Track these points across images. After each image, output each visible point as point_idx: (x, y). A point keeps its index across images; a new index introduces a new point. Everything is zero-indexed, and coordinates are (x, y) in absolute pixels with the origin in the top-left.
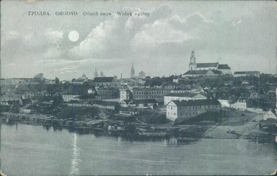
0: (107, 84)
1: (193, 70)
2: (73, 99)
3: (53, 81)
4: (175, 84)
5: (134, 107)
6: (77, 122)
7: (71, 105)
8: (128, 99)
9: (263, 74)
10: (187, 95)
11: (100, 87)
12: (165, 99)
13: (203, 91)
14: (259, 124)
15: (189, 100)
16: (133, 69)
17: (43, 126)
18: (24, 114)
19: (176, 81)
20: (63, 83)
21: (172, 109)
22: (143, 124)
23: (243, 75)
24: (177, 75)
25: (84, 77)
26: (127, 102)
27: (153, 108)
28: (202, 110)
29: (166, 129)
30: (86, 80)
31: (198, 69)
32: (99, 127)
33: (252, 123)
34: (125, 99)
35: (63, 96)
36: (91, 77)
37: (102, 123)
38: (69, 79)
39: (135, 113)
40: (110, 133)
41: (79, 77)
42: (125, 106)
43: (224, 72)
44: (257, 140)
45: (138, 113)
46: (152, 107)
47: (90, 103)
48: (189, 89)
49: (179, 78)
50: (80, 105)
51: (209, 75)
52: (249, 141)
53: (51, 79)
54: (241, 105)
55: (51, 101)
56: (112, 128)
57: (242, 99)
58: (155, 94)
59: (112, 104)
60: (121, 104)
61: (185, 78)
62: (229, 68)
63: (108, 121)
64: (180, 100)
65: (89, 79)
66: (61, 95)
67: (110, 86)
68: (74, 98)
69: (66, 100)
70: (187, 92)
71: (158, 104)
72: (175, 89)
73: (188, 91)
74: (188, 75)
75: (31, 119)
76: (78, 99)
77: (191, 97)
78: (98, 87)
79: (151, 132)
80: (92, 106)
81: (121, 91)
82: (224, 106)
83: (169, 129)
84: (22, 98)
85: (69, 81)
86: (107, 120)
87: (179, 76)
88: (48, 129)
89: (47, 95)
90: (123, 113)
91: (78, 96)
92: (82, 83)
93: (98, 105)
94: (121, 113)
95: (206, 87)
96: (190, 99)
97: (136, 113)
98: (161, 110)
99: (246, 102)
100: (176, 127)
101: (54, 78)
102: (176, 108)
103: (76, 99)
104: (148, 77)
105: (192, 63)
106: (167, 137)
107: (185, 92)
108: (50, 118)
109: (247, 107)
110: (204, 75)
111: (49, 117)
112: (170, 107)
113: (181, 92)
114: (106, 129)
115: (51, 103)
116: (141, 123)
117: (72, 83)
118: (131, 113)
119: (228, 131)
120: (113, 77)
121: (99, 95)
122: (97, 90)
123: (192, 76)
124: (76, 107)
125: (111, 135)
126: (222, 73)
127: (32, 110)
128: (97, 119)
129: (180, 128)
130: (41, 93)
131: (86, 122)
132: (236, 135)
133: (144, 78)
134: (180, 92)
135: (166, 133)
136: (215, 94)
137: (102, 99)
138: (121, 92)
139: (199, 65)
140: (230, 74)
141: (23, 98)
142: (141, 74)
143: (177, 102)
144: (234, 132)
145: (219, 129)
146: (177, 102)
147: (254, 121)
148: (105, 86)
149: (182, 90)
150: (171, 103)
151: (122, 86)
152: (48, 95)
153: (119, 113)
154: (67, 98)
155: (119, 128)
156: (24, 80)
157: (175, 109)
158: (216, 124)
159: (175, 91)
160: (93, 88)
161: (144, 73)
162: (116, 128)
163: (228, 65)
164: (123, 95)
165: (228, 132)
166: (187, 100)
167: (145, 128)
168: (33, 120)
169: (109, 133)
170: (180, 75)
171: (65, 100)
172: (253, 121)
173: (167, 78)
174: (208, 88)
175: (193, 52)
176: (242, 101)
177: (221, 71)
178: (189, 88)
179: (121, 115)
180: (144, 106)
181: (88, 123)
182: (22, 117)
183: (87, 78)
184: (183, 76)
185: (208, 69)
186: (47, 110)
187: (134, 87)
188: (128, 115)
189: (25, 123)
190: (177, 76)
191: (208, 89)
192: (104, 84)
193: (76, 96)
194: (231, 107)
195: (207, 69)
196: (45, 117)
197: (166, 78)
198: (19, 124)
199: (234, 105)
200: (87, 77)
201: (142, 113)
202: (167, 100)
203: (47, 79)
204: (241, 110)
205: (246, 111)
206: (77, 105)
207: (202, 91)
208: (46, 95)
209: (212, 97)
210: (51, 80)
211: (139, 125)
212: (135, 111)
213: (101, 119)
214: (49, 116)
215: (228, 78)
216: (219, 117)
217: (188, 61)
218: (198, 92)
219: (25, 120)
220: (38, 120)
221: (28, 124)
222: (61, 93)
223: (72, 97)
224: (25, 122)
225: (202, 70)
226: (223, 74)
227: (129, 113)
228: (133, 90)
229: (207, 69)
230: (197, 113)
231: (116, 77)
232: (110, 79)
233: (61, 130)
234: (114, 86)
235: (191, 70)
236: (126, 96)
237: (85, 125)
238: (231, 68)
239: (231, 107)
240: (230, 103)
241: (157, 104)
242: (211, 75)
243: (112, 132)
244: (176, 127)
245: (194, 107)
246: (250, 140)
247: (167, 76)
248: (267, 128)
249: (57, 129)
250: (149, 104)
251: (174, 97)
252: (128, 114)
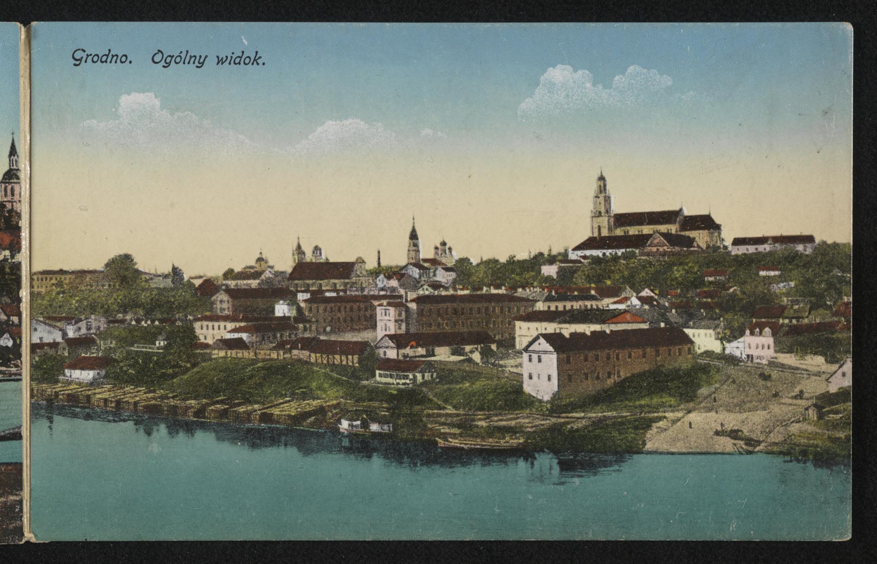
0: (335, 284)
1: (603, 235)
2: (229, 336)
3: (166, 276)
4: (549, 279)
5: (422, 356)
6: (242, 409)
7: (222, 354)
8: (399, 332)
9: (824, 243)
11: (313, 293)
12: (517, 328)
13: (635, 301)
14: (815, 405)
15: (593, 333)
16: (414, 236)
17: (136, 424)
18: (71, 387)
19: (550, 271)
20: (197, 283)
21: (540, 361)
22: (450, 410)
23: (761, 248)
24: (554, 253)
25: (262, 263)
26: (399, 341)
27: (482, 359)
28: (632, 364)
29: (522, 427)
30: (268, 274)
31: (619, 232)
32: (312, 425)
33: (795, 401)
34: (392, 332)
35: (197, 325)
37: (321, 411)
38: (215, 271)
39: (423, 377)
40: (346, 443)
41: (243, 266)
42: (392, 354)
43: (701, 238)
44: (811, 457)
45: (435, 375)
46: (477, 357)
47: (281, 346)
48: (593, 298)
49: (561, 261)
50: (248, 355)
52: (785, 462)
53: (159, 273)
54: (756, 346)
55: (157, 342)
56: (351, 426)
57: (762, 327)
59: (347, 348)
60: (380, 347)
61: (580, 262)
62: (718, 227)
63: (338, 404)
64: (566, 334)
65: (277, 268)
66: (191, 322)
67: (345, 291)
69: (205, 338)
70: (586, 306)
71: (498, 348)
72: (549, 299)
73: (588, 304)
74: (588, 253)
75: (94, 400)
76: (244, 336)
77: (603, 322)
78: (307, 296)
79: (476, 436)
80: (288, 356)
81: (379, 305)
82: (702, 350)
83: (531, 427)
84: (64, 334)
85: (217, 278)
86: (335, 402)
87: (560, 254)
88: (149, 433)
89: (146, 322)
90: (386, 376)
91: (243, 324)
92: (254, 283)
93: (307, 353)
94: (381, 378)
95: (647, 290)
96: (597, 327)
97: (427, 376)
98: (505, 366)
99: (774, 334)
100: (554, 420)
101: (168, 269)
102: (554, 356)
103: (236, 336)
104: (463, 261)
105: (600, 212)
106: (526, 453)
108: (154, 398)
109: (776, 351)
110: (637, 251)
111: (150, 395)
112: (535, 357)
113: (568, 307)
114: (336, 431)
115: (158, 348)
116: (444, 408)
117: (224, 282)
118: (411, 377)
119: (719, 428)
121: (309, 321)
122: (303, 305)
123: (601, 255)
124: (236, 361)
125: (348, 450)
126: (695, 244)
127: (98, 374)
128: (304, 397)
129: (568, 423)
130: (128, 317)
131: (271, 407)
132: (742, 442)
133: (450, 263)
134: (565, 307)
135: (522, 441)
136: (674, 311)
137: (318, 333)
138: (379, 311)
139: (623, 220)
140: (719, 247)
141: (71, 334)
142: (440, 252)
143: (554, 339)
144: (739, 431)
145: (690, 424)
146: (554, 339)
147: (800, 395)
148: (328, 291)
149: (570, 300)
150: (537, 342)
151: (382, 289)
152: (149, 322)
153: (374, 376)
154: (209, 333)
155: (374, 427)
156: (73, 277)
157: (551, 361)
158: (682, 406)
159: (547, 304)
161: (450, 249)
162: (365, 425)
163: (713, 216)
164: (387, 321)
165: (717, 433)
166: (588, 333)
167: (459, 426)
168: (102, 404)
169: (343, 444)
170: (562, 251)
171: (202, 338)
172: (795, 397)
173: (524, 261)
174: (652, 291)
175: (602, 178)
176: (761, 333)
177: (691, 236)
178: (593, 292)
179: (379, 383)
180: (453, 354)
181: (276, 411)
182: (68, 395)
183: (272, 267)
184: (573, 256)
185: (651, 232)
186: (147, 373)
187: (421, 292)
188: (404, 384)
189: (75, 416)
190: (554, 256)
191: (652, 294)
192: (326, 284)
193: (238, 325)
194: (727, 352)
195: (646, 230)
196: (137, 395)
197: (518, 261)
198: (56, 418)
199: (735, 344)
200: (270, 264)
201: (445, 374)
203: (146, 273)
204: (758, 361)
205: (772, 364)
206: (240, 355)
207: (634, 303)
208: (143, 323)
209: (667, 322)
210: (159, 276)
211: (439, 415)
212: (422, 372)
213: (318, 398)
214: (154, 391)
215: (716, 258)
216: (687, 383)
217: (588, 207)
219: (77, 405)
220: (118, 402)
221: (88, 417)
222: (190, 317)
223: (225, 329)
224: (78, 410)
225: (631, 233)
226: (698, 246)
227: (406, 377)
228: (417, 303)
229: (646, 230)
231: (363, 262)
232: (344, 270)
233: (193, 435)
234: (357, 290)
235: (596, 235)
236: (396, 321)
237: (266, 418)
238: (722, 228)
239: (727, 352)
240: (722, 339)
241: (494, 347)
242: (661, 249)
243: (352, 436)
244: (554, 420)
245: (609, 354)
246: (788, 458)
247: (522, 255)
248: (841, 418)
249: (177, 433)
250: (468, 348)
251: (545, 324)
252: (403, 381)
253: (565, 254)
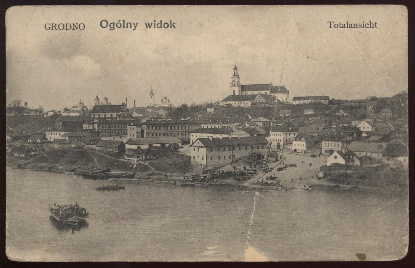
2: (61, 138)
20: (50, 114)
23: (306, 101)
35: (47, 133)
36: (90, 105)
38: (59, 108)
51: (258, 101)
55: (29, 141)
58: (178, 131)
68: (62, 136)
93: (95, 146)
96: (226, 136)
103: (64, 138)
120: (121, 104)
202: (194, 137)
230: (234, 156)
253: (218, 103)
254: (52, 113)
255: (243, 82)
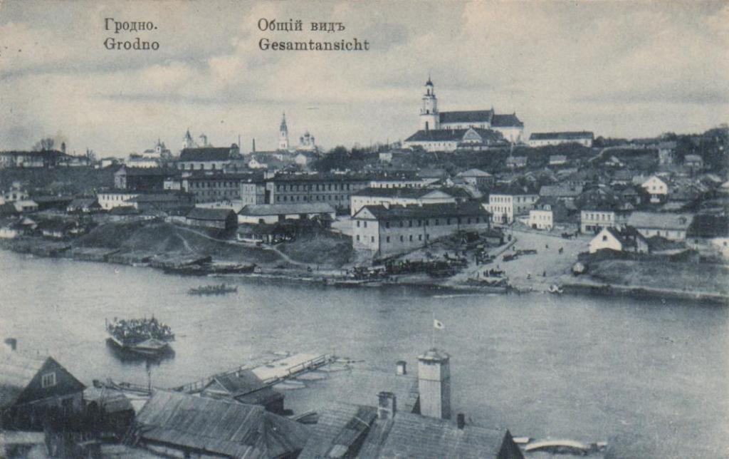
10: (406, 192)
36: (176, 149)
68: (128, 201)
107: (407, 185)
139: (444, 117)
160: (177, 177)
185: (468, 127)
218: (439, 186)
254: (109, 163)
255: (442, 108)
